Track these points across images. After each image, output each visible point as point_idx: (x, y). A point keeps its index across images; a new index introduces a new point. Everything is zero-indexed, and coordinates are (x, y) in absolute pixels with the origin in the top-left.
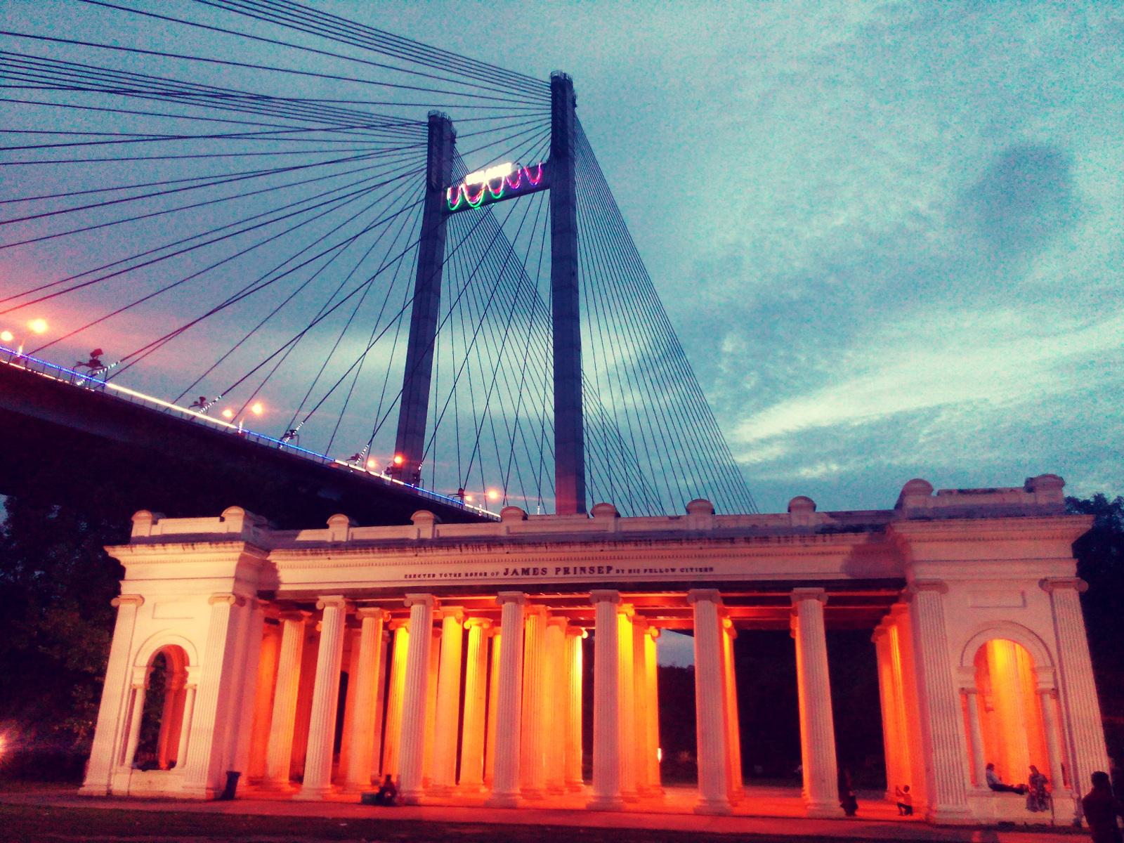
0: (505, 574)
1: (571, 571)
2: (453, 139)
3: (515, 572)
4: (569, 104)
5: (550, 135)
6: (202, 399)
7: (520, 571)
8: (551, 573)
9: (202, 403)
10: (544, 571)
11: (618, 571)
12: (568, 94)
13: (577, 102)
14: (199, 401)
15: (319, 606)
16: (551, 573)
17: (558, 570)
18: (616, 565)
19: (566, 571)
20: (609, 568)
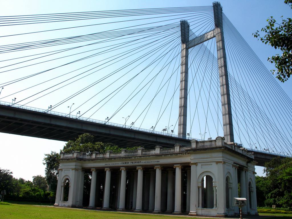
0: (122, 164)
1: (133, 163)
2: (189, 26)
3: (124, 163)
5: (214, 21)
7: (124, 163)
8: (130, 163)
10: (129, 163)
12: (219, 7)
13: (222, 9)
15: (91, 171)
16: (130, 163)
17: (131, 163)
18: (142, 161)
19: (133, 163)
20: (140, 162)
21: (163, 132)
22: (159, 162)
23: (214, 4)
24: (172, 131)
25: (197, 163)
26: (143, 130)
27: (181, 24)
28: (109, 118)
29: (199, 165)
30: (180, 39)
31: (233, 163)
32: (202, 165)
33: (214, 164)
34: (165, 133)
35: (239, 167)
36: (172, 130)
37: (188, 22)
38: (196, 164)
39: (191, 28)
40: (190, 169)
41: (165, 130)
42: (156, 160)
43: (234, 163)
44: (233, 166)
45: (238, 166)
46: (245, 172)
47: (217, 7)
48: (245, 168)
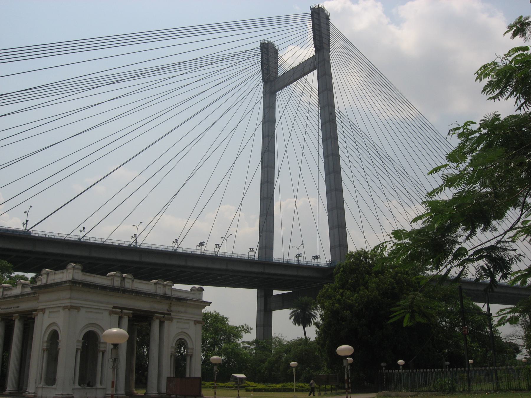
4: (323, 20)
6: (84, 228)
9: (84, 230)
11: (2, 309)
12: (322, 15)
14: (82, 229)
21: (199, 248)
22: (18, 308)
23: (312, 10)
24: (217, 246)
25: (45, 309)
26: (149, 247)
27: (261, 49)
28: (86, 231)
29: (47, 312)
30: (260, 75)
31: (111, 309)
32: (50, 312)
33: (61, 310)
34: (199, 251)
35: (132, 313)
36: (216, 245)
37: (276, 44)
38: (43, 310)
39: (280, 54)
40: (34, 322)
41: (201, 244)
42: (16, 305)
43: (114, 307)
44: (111, 313)
45: (131, 312)
46: (161, 323)
47: (319, 14)
48: (156, 315)
